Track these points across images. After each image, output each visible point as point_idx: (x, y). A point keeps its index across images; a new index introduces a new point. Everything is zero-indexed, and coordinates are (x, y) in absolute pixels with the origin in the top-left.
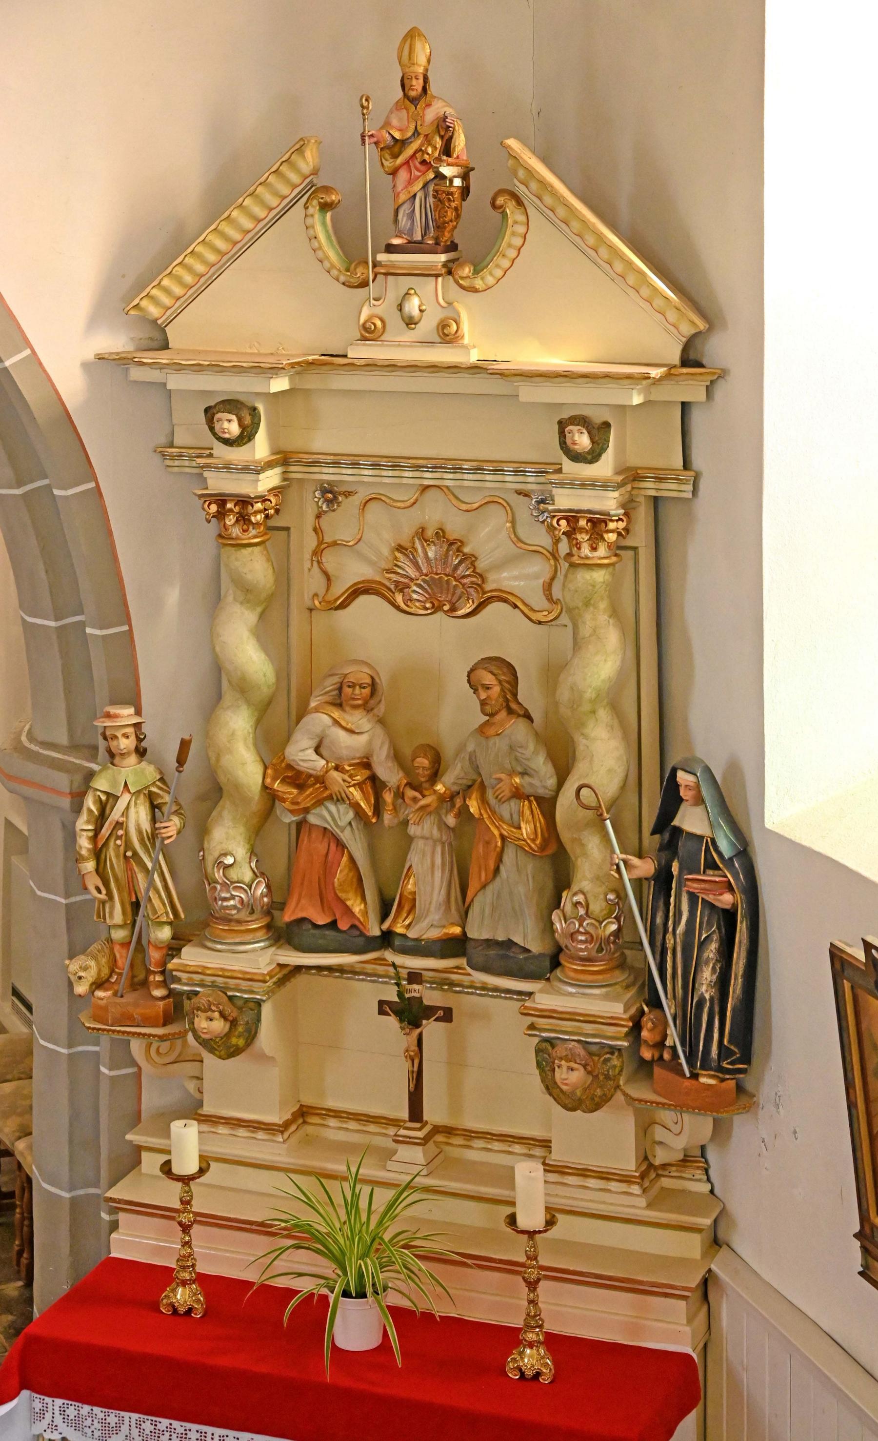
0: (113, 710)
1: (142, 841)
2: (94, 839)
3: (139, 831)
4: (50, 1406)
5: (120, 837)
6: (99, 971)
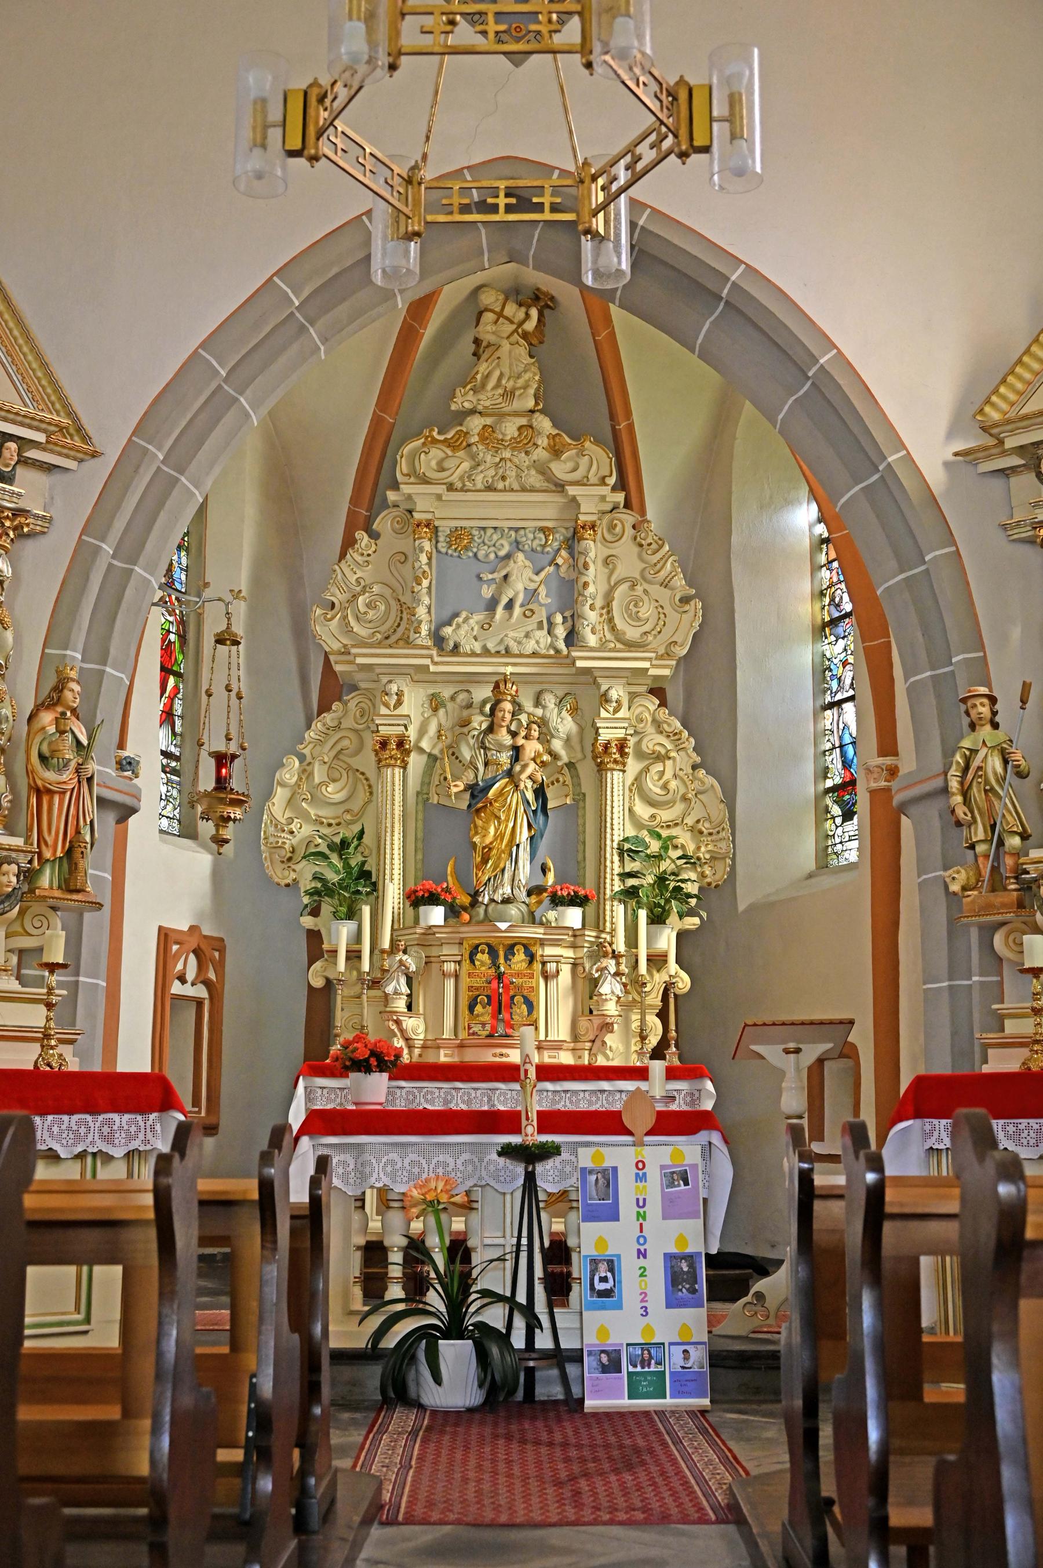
0: (972, 688)
1: (997, 781)
2: (962, 783)
3: (995, 773)
4: (937, 1127)
5: (981, 776)
6: (968, 878)
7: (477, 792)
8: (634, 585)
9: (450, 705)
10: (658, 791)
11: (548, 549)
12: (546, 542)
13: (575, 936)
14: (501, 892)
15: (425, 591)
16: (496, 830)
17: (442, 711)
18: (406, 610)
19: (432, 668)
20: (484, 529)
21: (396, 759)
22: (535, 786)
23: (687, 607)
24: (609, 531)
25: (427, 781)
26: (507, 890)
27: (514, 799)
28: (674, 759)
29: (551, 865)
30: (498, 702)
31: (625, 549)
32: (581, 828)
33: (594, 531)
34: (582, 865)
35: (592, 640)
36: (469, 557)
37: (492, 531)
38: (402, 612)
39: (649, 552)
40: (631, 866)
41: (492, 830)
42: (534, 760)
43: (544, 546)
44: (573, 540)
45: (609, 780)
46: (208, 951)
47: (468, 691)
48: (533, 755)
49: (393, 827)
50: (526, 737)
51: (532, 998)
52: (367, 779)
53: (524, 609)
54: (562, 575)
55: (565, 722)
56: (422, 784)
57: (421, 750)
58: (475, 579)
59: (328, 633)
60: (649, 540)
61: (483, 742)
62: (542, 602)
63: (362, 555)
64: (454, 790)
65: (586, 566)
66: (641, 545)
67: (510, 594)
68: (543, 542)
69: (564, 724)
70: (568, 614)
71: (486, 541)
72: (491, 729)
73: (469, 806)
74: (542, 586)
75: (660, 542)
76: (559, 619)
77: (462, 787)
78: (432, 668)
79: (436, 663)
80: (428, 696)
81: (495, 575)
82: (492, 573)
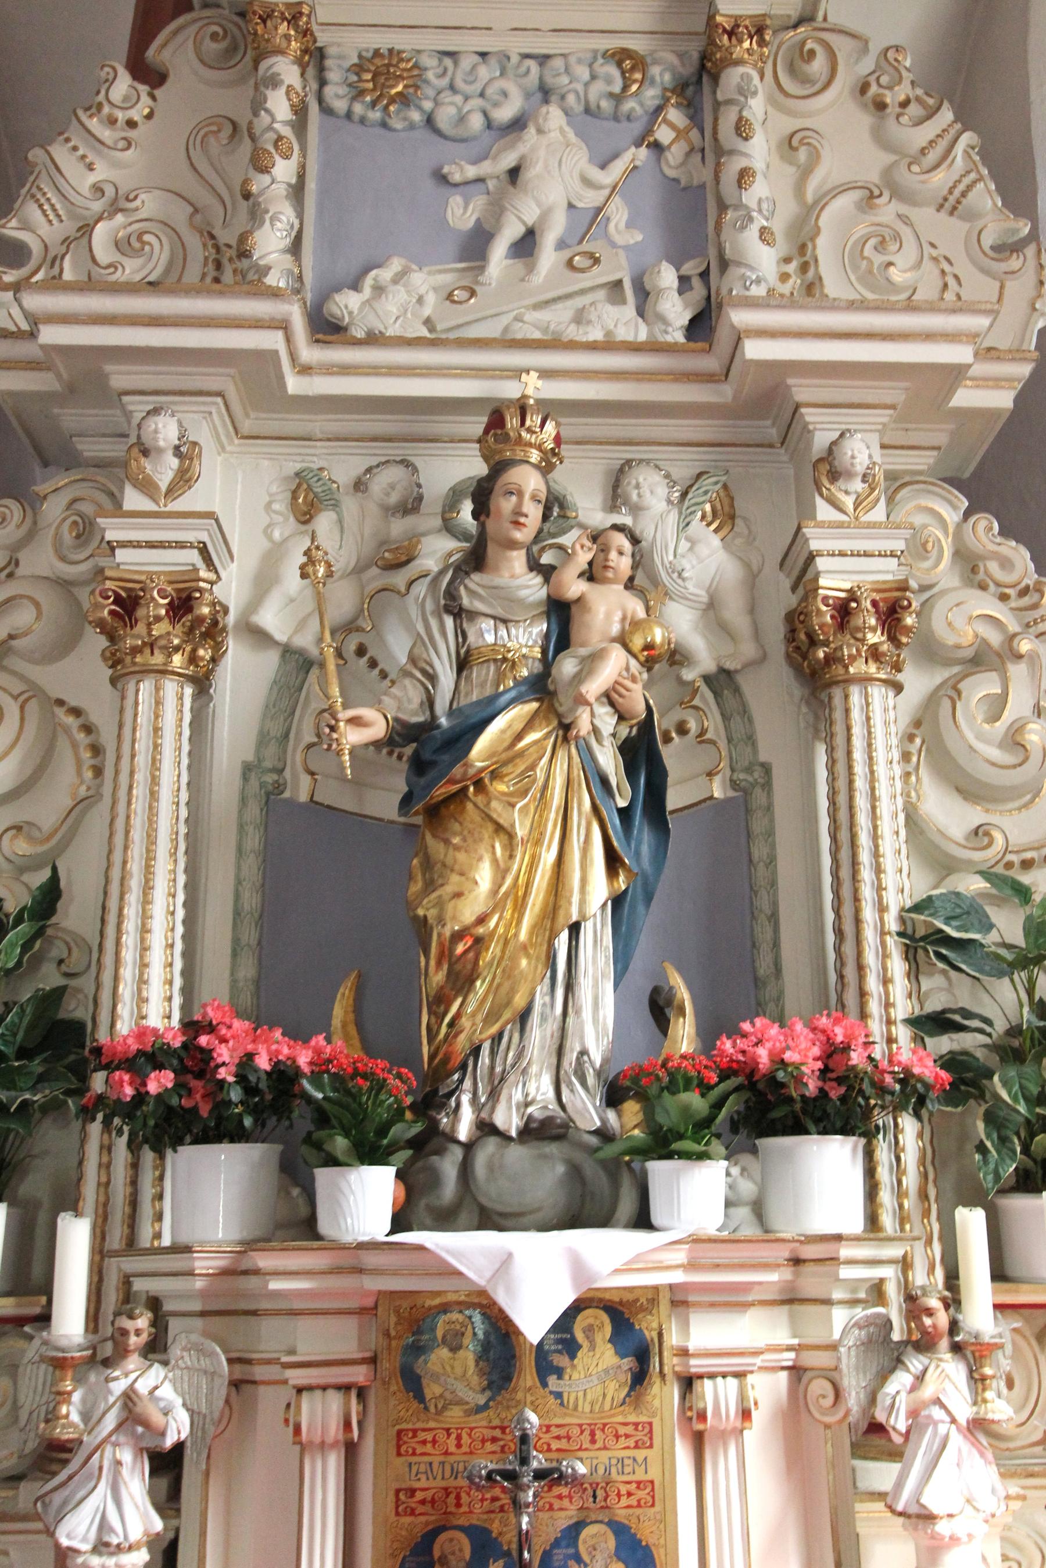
7: (431, 754)
8: (872, 196)
9: (350, 504)
10: (994, 753)
11: (629, 105)
12: (625, 88)
13: (797, 1261)
14: (518, 1096)
15: (280, 190)
16: (500, 873)
17: (324, 522)
19: (294, 384)
20: (451, 54)
21: (170, 651)
22: (624, 732)
23: (1015, 263)
24: (792, 70)
25: (276, 729)
26: (540, 1088)
27: (559, 770)
28: (1033, 659)
29: (683, 994)
30: (498, 468)
31: (835, 113)
32: (761, 870)
33: (762, 43)
34: (770, 991)
36: (412, 126)
37: (477, 59)
38: (218, 266)
39: (904, 119)
40: (941, 992)
41: (484, 875)
42: (622, 640)
43: (617, 99)
44: (700, 81)
45: (856, 715)
47: (406, 463)
48: (615, 629)
49: (148, 871)
50: (590, 575)
51: (647, 1533)
52: (88, 729)
53: (567, 254)
54: (671, 173)
55: (703, 550)
56: (263, 740)
57: (259, 636)
58: (428, 185)
60: (903, 91)
61: (451, 594)
62: (619, 240)
63: (112, 121)
64: (352, 737)
65: (743, 130)
66: (881, 106)
67: (530, 214)
68: (617, 88)
69: (700, 559)
70: (691, 268)
71: (459, 84)
72: (477, 558)
73: (407, 801)
74: (617, 201)
75: (931, 101)
76: (668, 277)
77: (378, 730)
78: (294, 384)
79: (305, 370)
80: (286, 479)
81: (486, 168)
82: (475, 162)
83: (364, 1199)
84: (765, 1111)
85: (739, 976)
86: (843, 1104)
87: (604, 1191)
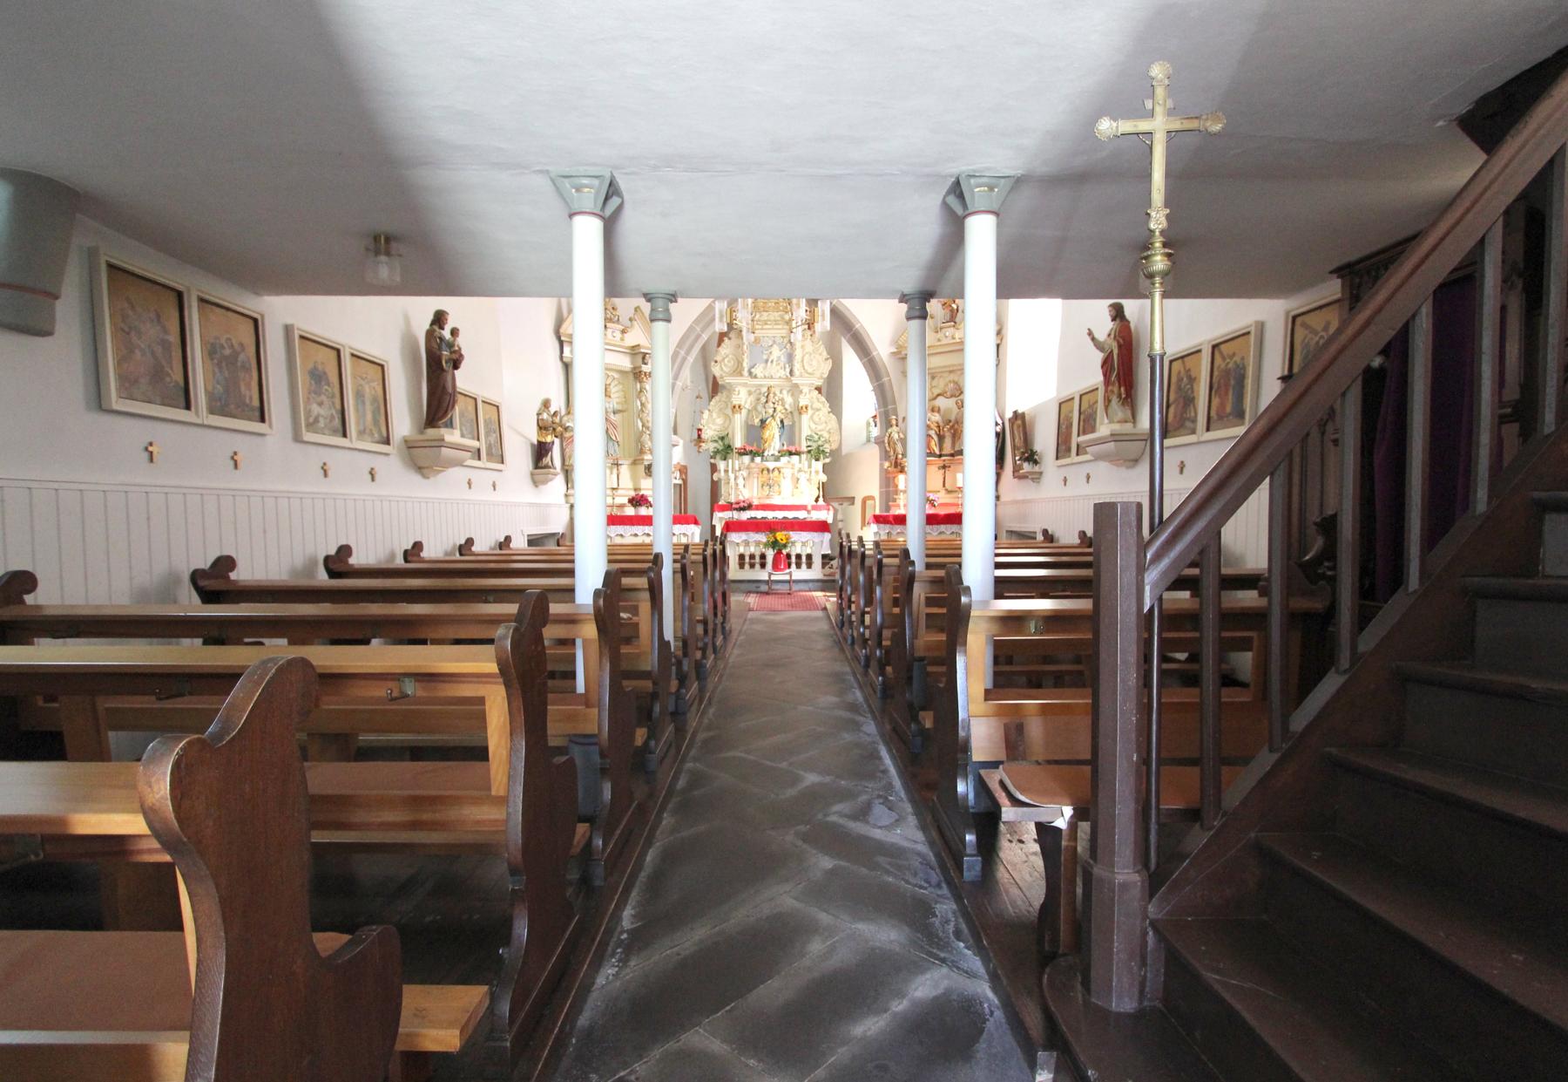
7: (763, 422)
18: (740, 363)
35: (797, 372)
46: (683, 470)
59: (716, 370)
69: (789, 400)
83: (758, 459)
84: (791, 454)
85: (791, 442)
86: (798, 453)
87: (777, 459)
